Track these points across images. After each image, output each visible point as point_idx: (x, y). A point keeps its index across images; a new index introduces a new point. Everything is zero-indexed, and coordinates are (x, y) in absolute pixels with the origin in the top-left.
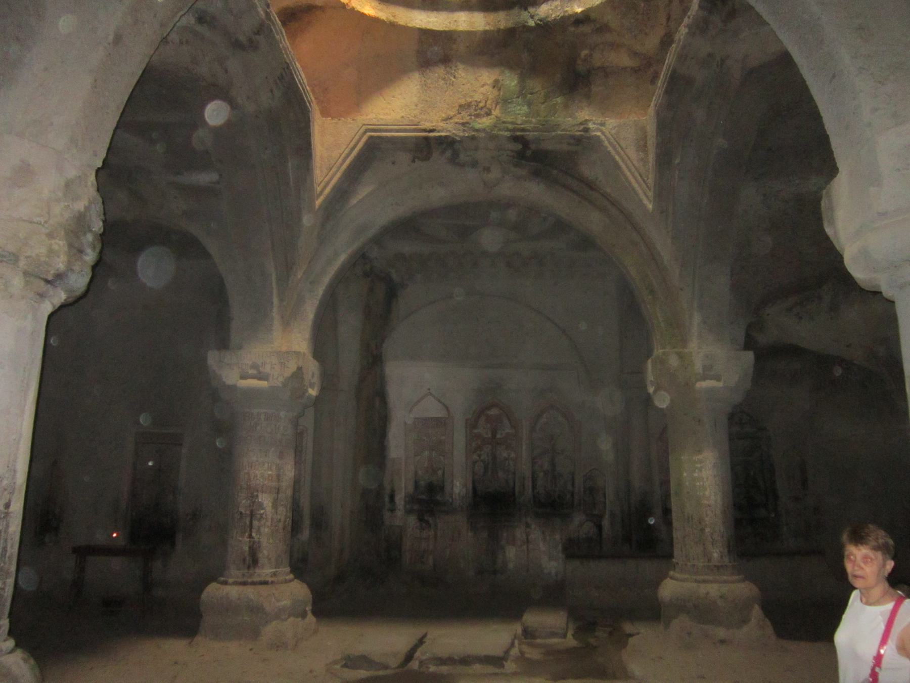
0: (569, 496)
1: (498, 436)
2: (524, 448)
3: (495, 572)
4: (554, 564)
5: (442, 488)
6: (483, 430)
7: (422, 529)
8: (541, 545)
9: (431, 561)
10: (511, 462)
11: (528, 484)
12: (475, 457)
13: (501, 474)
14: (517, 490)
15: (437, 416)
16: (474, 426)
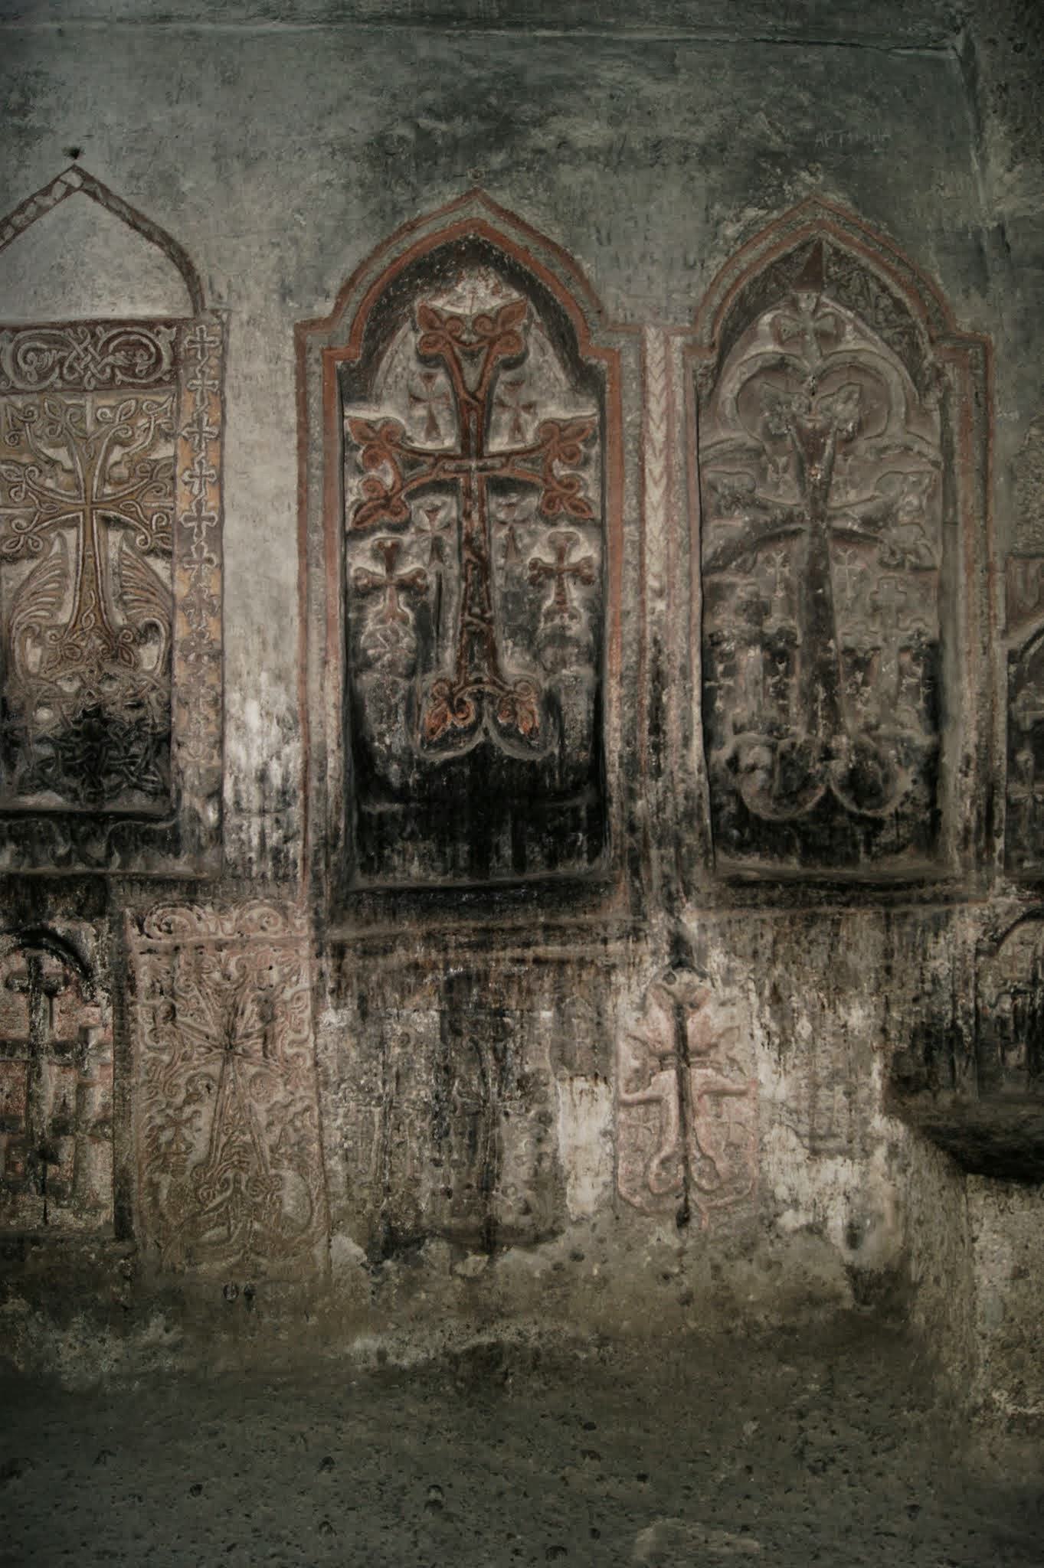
0: (906, 781)
1: (498, 444)
2: (655, 494)
3: (489, 1239)
4: (841, 1172)
5: (163, 742)
6: (404, 405)
7: (41, 988)
8: (764, 1071)
9: (100, 1179)
10: (576, 594)
11: (682, 707)
12: (363, 562)
13: (513, 662)
14: (614, 746)
15: (124, 311)
16: (355, 382)
